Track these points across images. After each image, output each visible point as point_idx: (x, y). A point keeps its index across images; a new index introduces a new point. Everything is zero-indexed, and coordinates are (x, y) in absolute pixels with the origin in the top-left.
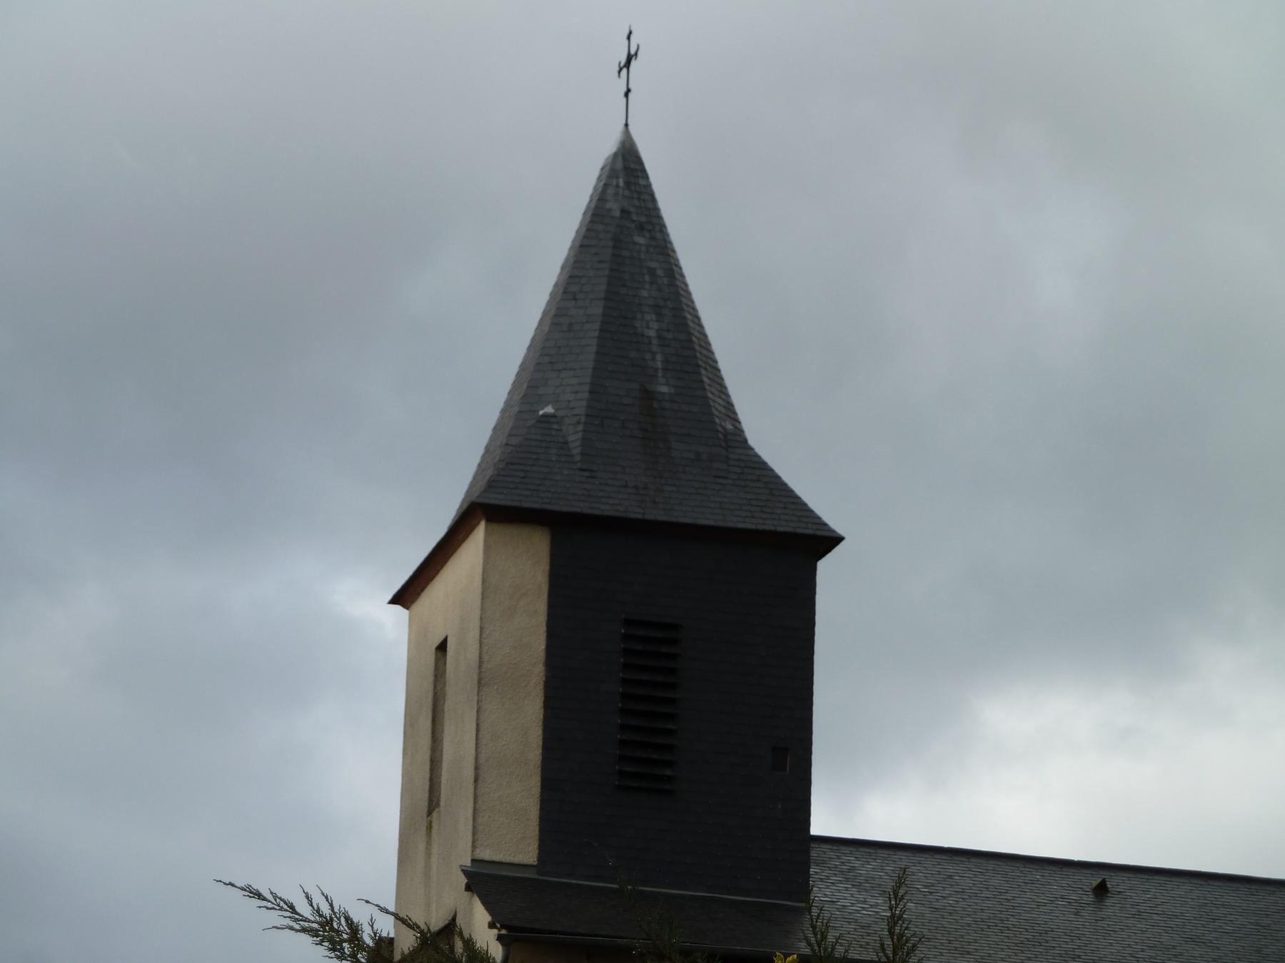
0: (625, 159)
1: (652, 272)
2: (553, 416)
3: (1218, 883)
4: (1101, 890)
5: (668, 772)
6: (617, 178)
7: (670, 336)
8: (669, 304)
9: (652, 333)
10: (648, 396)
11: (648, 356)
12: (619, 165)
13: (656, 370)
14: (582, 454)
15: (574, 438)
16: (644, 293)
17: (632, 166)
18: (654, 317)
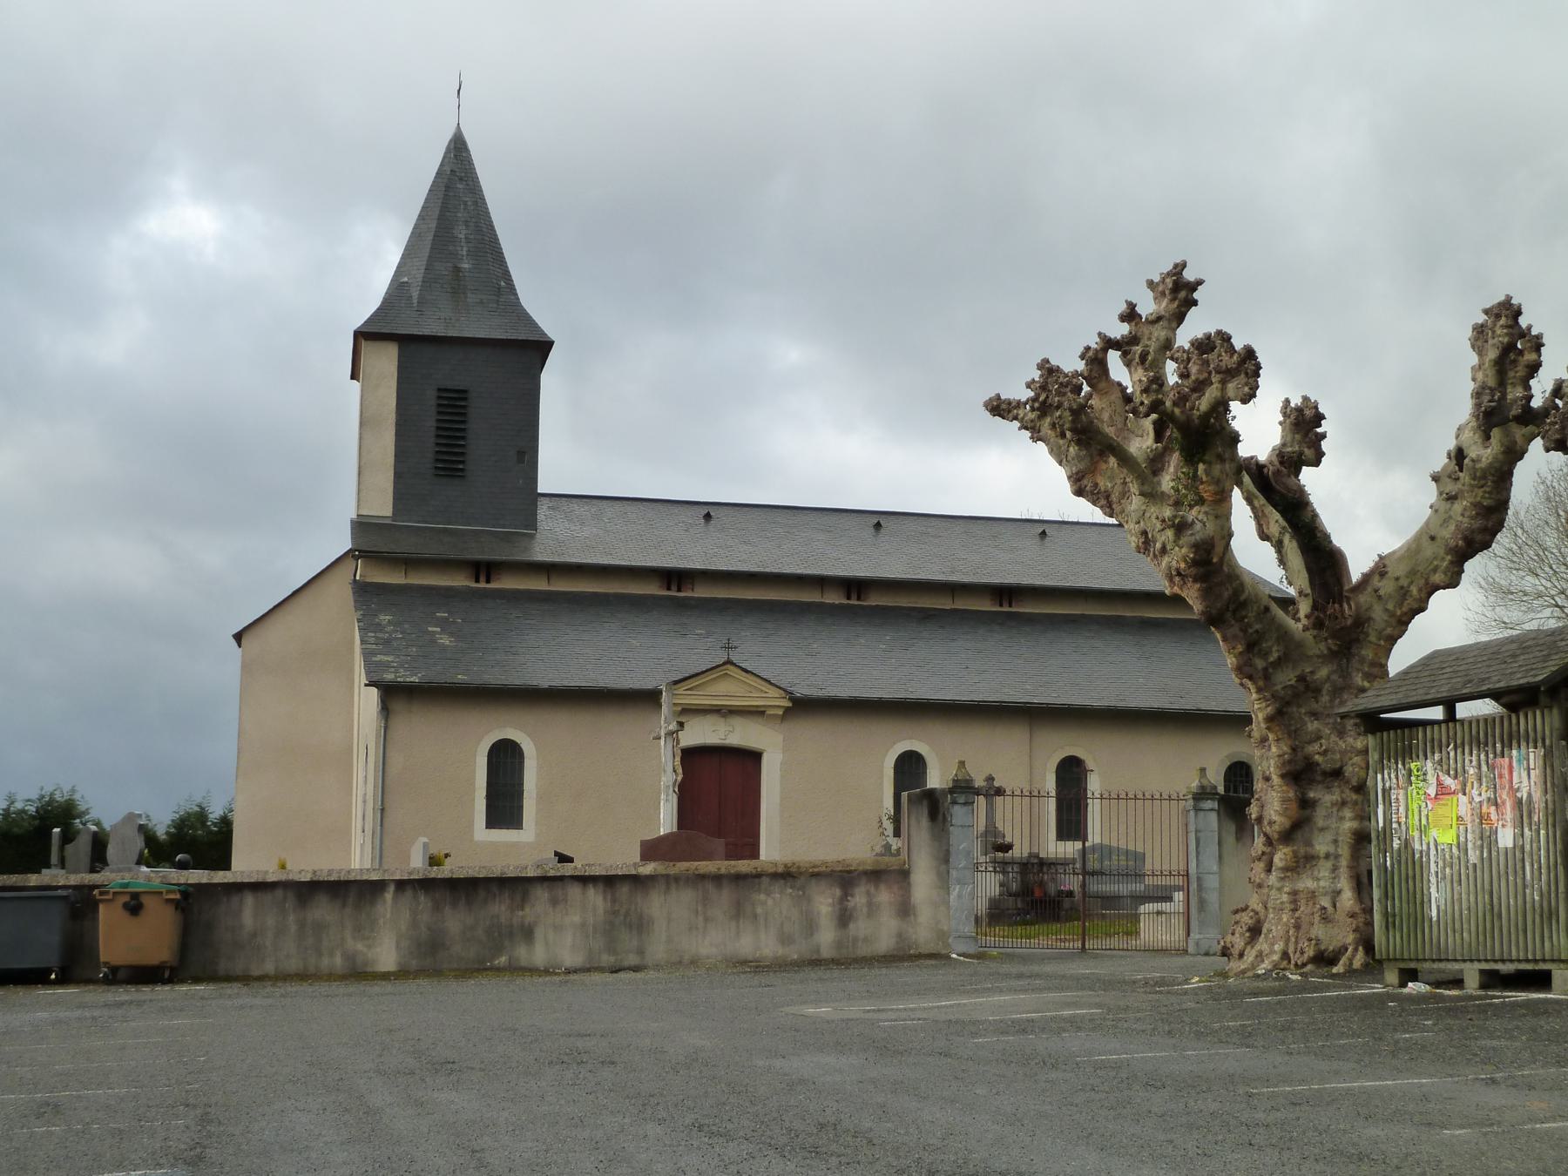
0: (455, 143)
1: (465, 203)
2: (407, 283)
3: (983, 522)
4: (708, 517)
5: (461, 467)
6: (450, 153)
7: (472, 237)
8: (474, 220)
9: (462, 236)
10: (457, 270)
11: (459, 248)
12: (452, 146)
13: (463, 256)
14: (418, 302)
15: (415, 294)
16: (460, 215)
17: (459, 146)
18: (464, 227)
